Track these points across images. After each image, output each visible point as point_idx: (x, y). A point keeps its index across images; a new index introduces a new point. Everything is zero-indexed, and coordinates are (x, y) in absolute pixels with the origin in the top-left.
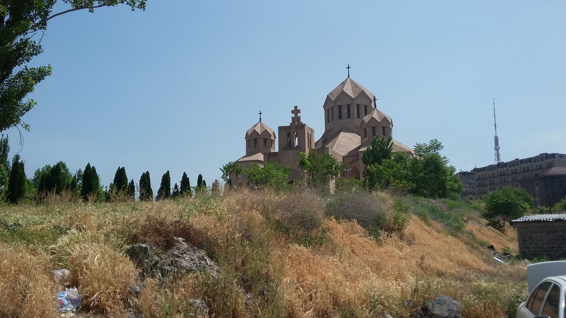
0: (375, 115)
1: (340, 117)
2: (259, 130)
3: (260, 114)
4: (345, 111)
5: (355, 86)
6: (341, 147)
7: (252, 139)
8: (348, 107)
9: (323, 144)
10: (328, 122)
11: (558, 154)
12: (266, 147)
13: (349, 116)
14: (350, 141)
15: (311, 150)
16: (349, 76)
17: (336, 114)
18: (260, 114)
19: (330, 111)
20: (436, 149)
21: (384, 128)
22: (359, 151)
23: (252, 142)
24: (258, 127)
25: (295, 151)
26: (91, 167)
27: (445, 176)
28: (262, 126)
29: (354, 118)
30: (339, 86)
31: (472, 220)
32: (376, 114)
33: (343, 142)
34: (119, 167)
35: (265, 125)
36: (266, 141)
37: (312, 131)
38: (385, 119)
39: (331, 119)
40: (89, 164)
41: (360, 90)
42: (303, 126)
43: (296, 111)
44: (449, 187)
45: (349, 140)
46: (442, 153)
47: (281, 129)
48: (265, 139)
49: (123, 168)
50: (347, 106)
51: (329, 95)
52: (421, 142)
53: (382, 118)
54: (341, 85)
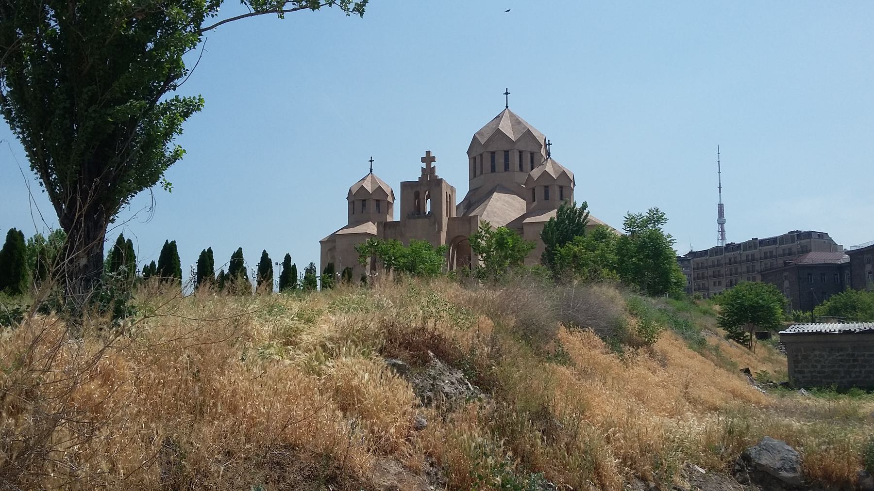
0: (549, 168)
1: (493, 170)
2: (369, 187)
3: (371, 161)
4: (500, 160)
5: (516, 122)
6: (495, 216)
9: (466, 210)
10: (475, 176)
12: (379, 212)
13: (506, 168)
15: (450, 219)
16: (507, 107)
17: (487, 165)
18: (370, 162)
20: (656, 224)
21: (561, 187)
23: (358, 205)
24: (368, 181)
26: (126, 240)
27: (670, 264)
28: (374, 181)
29: (514, 171)
30: (492, 121)
31: (707, 330)
33: (498, 209)
34: (167, 241)
35: (378, 178)
37: (452, 189)
38: (564, 174)
42: (440, 182)
43: (428, 159)
44: (674, 281)
45: (507, 205)
46: (665, 229)
47: (405, 186)
48: (378, 201)
49: (174, 243)
50: (503, 153)
51: (477, 136)
52: (635, 212)
54: (495, 119)
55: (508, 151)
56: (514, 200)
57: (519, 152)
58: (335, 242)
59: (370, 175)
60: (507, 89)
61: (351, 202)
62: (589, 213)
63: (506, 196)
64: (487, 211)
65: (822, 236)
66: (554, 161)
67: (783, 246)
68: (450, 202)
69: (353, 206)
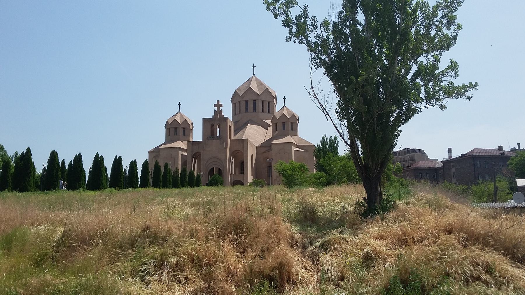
2: (179, 120)
3: (179, 104)
4: (251, 106)
5: (260, 84)
7: (172, 127)
8: (253, 102)
10: (236, 114)
11: (418, 149)
12: (176, 135)
14: (256, 133)
15: (231, 140)
17: (243, 108)
18: (179, 105)
19: (238, 105)
21: (292, 123)
23: (172, 131)
26: (100, 156)
28: (182, 116)
29: (259, 112)
30: (246, 82)
33: (251, 134)
34: (116, 156)
35: (184, 115)
36: (185, 130)
39: (238, 112)
40: (97, 153)
45: (256, 132)
47: (205, 120)
48: (184, 128)
49: (120, 157)
50: (253, 101)
51: (237, 90)
53: (291, 115)
56: (259, 129)
57: (262, 101)
58: (159, 152)
59: (179, 113)
61: (168, 129)
62: (338, 142)
64: (245, 135)
65: (421, 151)
67: (400, 157)
68: (231, 131)
69: (168, 131)
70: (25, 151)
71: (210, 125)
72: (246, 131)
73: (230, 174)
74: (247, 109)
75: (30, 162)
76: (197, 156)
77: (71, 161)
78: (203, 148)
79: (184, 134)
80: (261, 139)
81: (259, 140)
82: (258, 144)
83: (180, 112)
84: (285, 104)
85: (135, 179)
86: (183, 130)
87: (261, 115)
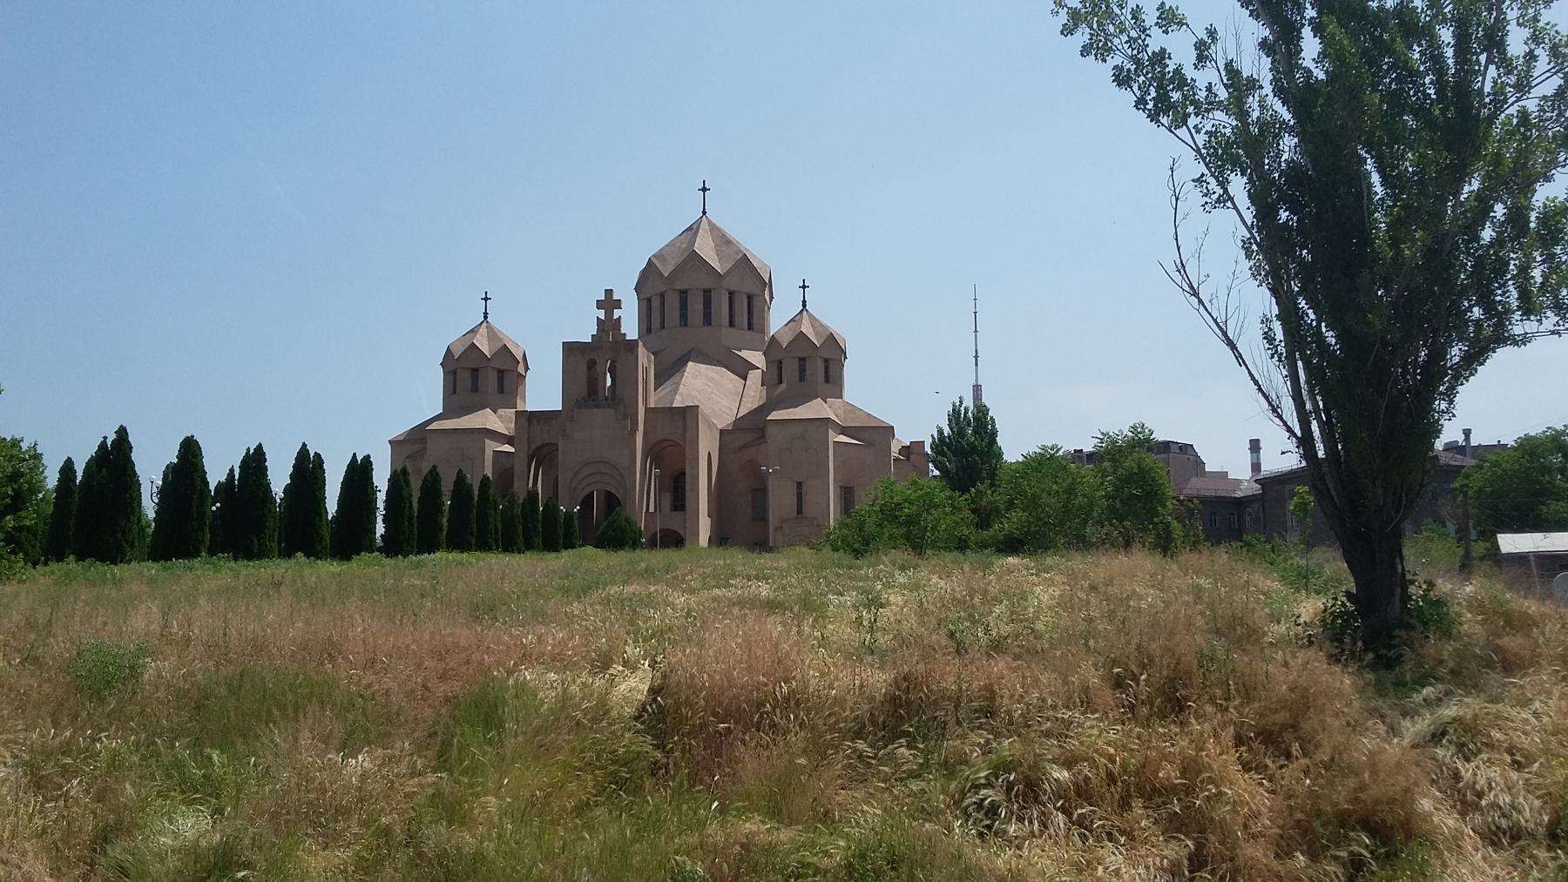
2: (485, 347)
3: (486, 299)
4: (696, 306)
5: (723, 241)
8: (704, 296)
10: (649, 331)
16: (704, 213)
17: (673, 312)
19: (656, 304)
21: (826, 361)
22: (768, 418)
23: (465, 380)
24: (482, 336)
25: (612, 411)
26: (312, 455)
28: (493, 334)
29: (721, 326)
32: (807, 324)
34: (355, 454)
40: (304, 445)
41: (737, 253)
45: (712, 385)
47: (570, 349)
48: (501, 372)
49: (367, 459)
50: (702, 293)
51: (654, 260)
54: (685, 234)
55: (710, 291)
56: (721, 376)
58: (426, 443)
59: (484, 324)
60: (704, 182)
61: (449, 372)
63: (707, 368)
64: (681, 395)
65: (1186, 449)
66: (811, 315)
70: (112, 437)
71: (585, 366)
72: (683, 382)
73: (644, 510)
74: (684, 316)
75: (129, 472)
76: (543, 455)
77: (232, 470)
78: (565, 431)
79: (501, 390)
80: (726, 407)
81: (724, 409)
82: (725, 420)
83: (487, 322)
84: (804, 303)
85: (406, 524)
86: (498, 377)
87: (728, 335)
